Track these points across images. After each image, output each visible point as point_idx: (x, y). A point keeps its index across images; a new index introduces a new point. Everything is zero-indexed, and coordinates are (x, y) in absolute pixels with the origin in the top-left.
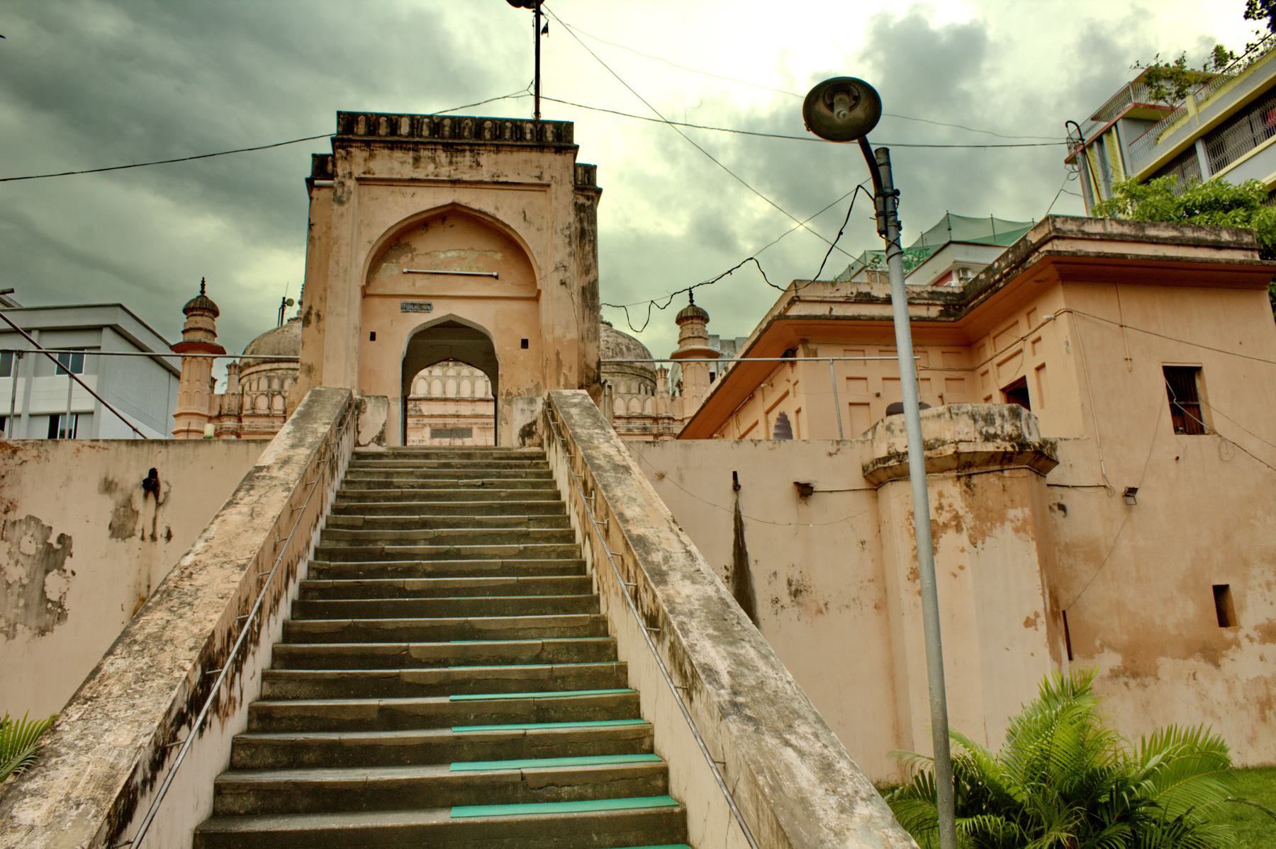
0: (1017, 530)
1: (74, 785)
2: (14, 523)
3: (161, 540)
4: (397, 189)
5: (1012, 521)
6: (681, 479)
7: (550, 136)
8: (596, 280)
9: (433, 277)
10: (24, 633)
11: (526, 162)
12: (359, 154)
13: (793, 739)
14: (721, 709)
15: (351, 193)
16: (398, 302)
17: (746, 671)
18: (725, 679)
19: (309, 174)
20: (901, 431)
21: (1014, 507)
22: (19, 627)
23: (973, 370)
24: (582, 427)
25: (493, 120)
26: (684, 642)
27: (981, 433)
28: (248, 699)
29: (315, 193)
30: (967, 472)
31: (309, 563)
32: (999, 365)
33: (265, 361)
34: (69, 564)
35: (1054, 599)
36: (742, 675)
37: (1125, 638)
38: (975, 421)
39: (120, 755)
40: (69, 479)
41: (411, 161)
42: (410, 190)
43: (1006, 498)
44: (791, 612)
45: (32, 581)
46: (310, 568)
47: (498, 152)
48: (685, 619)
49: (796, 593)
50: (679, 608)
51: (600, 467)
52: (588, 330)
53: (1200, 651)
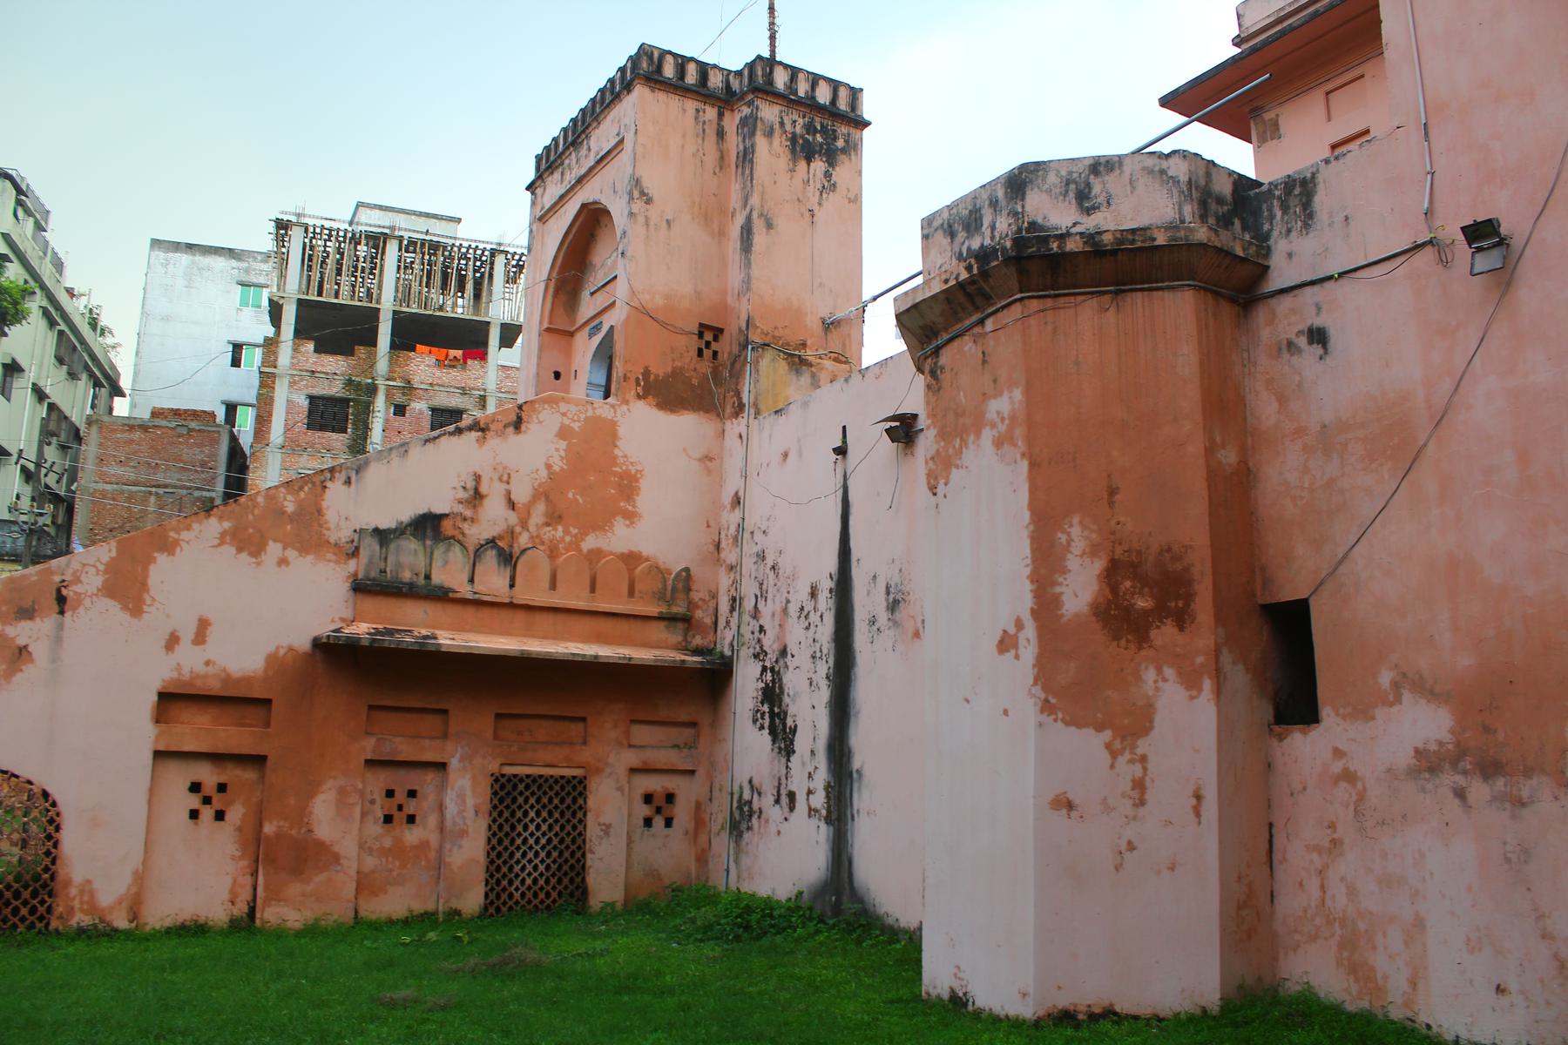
0: (998, 443)
5: (993, 426)
6: (800, 454)
21: (998, 394)
37: (1466, 661)
38: (952, 235)
44: (889, 635)
49: (893, 606)
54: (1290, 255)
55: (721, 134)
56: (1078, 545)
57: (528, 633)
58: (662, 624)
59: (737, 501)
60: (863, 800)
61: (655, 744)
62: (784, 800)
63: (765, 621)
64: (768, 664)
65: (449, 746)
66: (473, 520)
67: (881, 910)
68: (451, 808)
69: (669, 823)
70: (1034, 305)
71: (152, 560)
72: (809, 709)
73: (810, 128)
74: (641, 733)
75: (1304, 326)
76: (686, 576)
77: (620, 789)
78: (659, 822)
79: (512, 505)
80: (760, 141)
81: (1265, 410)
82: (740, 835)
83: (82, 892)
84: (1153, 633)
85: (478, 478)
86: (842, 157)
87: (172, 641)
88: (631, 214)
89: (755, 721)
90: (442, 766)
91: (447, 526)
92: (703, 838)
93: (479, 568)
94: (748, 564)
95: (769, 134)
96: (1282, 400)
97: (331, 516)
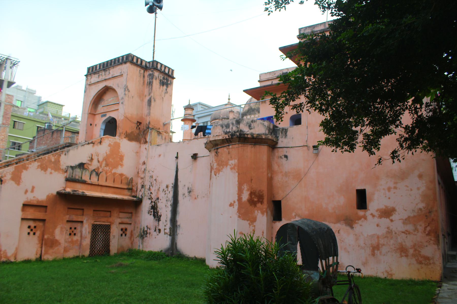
0: (231, 169)
5: (230, 165)
6: (164, 156)
7: (125, 59)
16: (101, 115)
21: (232, 160)
27: (224, 132)
30: (217, 147)
33: (213, 120)
37: (307, 213)
38: (222, 127)
49: (190, 192)
53: (344, 220)
54: (282, 141)
55: (144, 76)
56: (246, 189)
57: (101, 191)
58: (127, 190)
59: (144, 163)
60: (180, 232)
61: (124, 217)
62: (157, 231)
63: (152, 190)
64: (153, 201)
65: (84, 217)
66: (91, 165)
67: (185, 254)
68: (84, 232)
69: (126, 235)
70: (240, 145)
71: (22, 172)
72: (165, 211)
73: (164, 78)
74: (122, 215)
75: (284, 154)
76: (132, 180)
77: (117, 227)
78: (124, 235)
79: (99, 161)
80: (154, 80)
81: (275, 167)
82: (143, 238)
83: (4, 253)
84: (257, 205)
85: (92, 155)
86: (169, 86)
87: (26, 192)
88: (125, 94)
89: (149, 213)
90: (82, 222)
91: (85, 166)
92: (132, 239)
93: (92, 176)
94: (147, 178)
95: (156, 79)
96: (279, 166)
97: (62, 163)
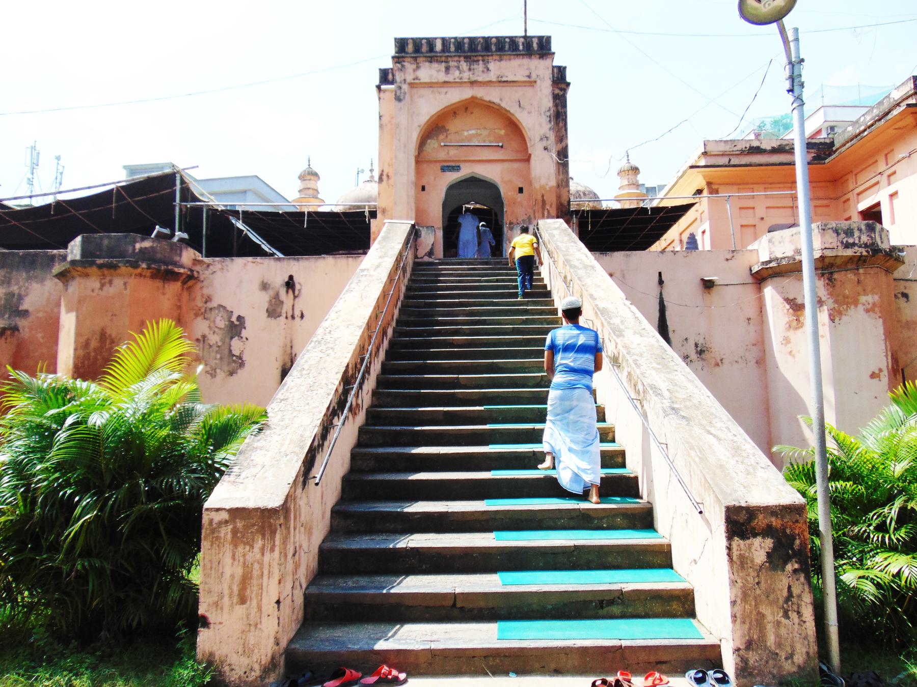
0: (867, 311)
1: (282, 445)
2: (211, 309)
3: (298, 319)
4: (435, 89)
6: (624, 277)
7: (535, 46)
8: (567, 146)
9: (460, 148)
10: (221, 375)
11: (520, 66)
12: (409, 66)
13: (712, 430)
14: (665, 411)
15: (405, 93)
17: (679, 389)
18: (666, 394)
19: (378, 83)
20: (780, 242)
22: (218, 371)
23: (837, 199)
24: (562, 242)
25: (497, 38)
26: (638, 371)
27: (842, 242)
28: (365, 407)
29: (382, 95)
31: (394, 329)
32: (859, 194)
34: (244, 333)
35: (895, 359)
36: (677, 391)
38: (838, 234)
39: (305, 430)
40: (241, 282)
41: (444, 69)
42: (444, 90)
43: (860, 289)
45: (224, 343)
46: (395, 331)
47: (501, 60)
48: (637, 358)
49: (701, 352)
50: (633, 351)
51: (575, 267)
52: (562, 180)
